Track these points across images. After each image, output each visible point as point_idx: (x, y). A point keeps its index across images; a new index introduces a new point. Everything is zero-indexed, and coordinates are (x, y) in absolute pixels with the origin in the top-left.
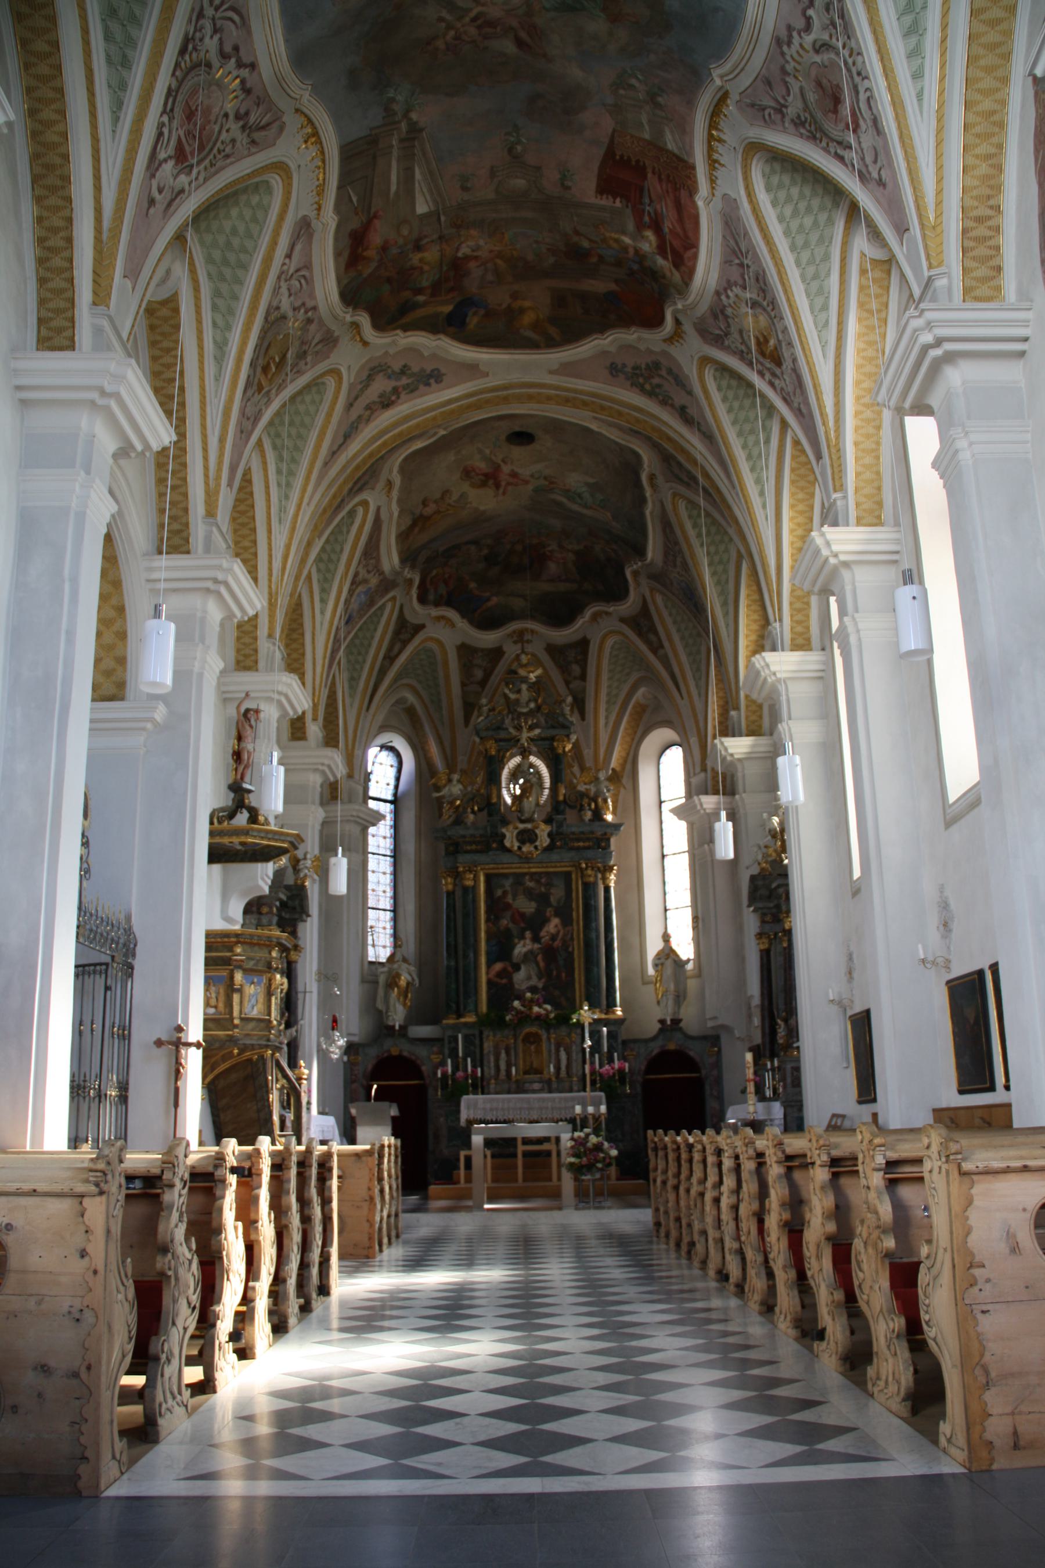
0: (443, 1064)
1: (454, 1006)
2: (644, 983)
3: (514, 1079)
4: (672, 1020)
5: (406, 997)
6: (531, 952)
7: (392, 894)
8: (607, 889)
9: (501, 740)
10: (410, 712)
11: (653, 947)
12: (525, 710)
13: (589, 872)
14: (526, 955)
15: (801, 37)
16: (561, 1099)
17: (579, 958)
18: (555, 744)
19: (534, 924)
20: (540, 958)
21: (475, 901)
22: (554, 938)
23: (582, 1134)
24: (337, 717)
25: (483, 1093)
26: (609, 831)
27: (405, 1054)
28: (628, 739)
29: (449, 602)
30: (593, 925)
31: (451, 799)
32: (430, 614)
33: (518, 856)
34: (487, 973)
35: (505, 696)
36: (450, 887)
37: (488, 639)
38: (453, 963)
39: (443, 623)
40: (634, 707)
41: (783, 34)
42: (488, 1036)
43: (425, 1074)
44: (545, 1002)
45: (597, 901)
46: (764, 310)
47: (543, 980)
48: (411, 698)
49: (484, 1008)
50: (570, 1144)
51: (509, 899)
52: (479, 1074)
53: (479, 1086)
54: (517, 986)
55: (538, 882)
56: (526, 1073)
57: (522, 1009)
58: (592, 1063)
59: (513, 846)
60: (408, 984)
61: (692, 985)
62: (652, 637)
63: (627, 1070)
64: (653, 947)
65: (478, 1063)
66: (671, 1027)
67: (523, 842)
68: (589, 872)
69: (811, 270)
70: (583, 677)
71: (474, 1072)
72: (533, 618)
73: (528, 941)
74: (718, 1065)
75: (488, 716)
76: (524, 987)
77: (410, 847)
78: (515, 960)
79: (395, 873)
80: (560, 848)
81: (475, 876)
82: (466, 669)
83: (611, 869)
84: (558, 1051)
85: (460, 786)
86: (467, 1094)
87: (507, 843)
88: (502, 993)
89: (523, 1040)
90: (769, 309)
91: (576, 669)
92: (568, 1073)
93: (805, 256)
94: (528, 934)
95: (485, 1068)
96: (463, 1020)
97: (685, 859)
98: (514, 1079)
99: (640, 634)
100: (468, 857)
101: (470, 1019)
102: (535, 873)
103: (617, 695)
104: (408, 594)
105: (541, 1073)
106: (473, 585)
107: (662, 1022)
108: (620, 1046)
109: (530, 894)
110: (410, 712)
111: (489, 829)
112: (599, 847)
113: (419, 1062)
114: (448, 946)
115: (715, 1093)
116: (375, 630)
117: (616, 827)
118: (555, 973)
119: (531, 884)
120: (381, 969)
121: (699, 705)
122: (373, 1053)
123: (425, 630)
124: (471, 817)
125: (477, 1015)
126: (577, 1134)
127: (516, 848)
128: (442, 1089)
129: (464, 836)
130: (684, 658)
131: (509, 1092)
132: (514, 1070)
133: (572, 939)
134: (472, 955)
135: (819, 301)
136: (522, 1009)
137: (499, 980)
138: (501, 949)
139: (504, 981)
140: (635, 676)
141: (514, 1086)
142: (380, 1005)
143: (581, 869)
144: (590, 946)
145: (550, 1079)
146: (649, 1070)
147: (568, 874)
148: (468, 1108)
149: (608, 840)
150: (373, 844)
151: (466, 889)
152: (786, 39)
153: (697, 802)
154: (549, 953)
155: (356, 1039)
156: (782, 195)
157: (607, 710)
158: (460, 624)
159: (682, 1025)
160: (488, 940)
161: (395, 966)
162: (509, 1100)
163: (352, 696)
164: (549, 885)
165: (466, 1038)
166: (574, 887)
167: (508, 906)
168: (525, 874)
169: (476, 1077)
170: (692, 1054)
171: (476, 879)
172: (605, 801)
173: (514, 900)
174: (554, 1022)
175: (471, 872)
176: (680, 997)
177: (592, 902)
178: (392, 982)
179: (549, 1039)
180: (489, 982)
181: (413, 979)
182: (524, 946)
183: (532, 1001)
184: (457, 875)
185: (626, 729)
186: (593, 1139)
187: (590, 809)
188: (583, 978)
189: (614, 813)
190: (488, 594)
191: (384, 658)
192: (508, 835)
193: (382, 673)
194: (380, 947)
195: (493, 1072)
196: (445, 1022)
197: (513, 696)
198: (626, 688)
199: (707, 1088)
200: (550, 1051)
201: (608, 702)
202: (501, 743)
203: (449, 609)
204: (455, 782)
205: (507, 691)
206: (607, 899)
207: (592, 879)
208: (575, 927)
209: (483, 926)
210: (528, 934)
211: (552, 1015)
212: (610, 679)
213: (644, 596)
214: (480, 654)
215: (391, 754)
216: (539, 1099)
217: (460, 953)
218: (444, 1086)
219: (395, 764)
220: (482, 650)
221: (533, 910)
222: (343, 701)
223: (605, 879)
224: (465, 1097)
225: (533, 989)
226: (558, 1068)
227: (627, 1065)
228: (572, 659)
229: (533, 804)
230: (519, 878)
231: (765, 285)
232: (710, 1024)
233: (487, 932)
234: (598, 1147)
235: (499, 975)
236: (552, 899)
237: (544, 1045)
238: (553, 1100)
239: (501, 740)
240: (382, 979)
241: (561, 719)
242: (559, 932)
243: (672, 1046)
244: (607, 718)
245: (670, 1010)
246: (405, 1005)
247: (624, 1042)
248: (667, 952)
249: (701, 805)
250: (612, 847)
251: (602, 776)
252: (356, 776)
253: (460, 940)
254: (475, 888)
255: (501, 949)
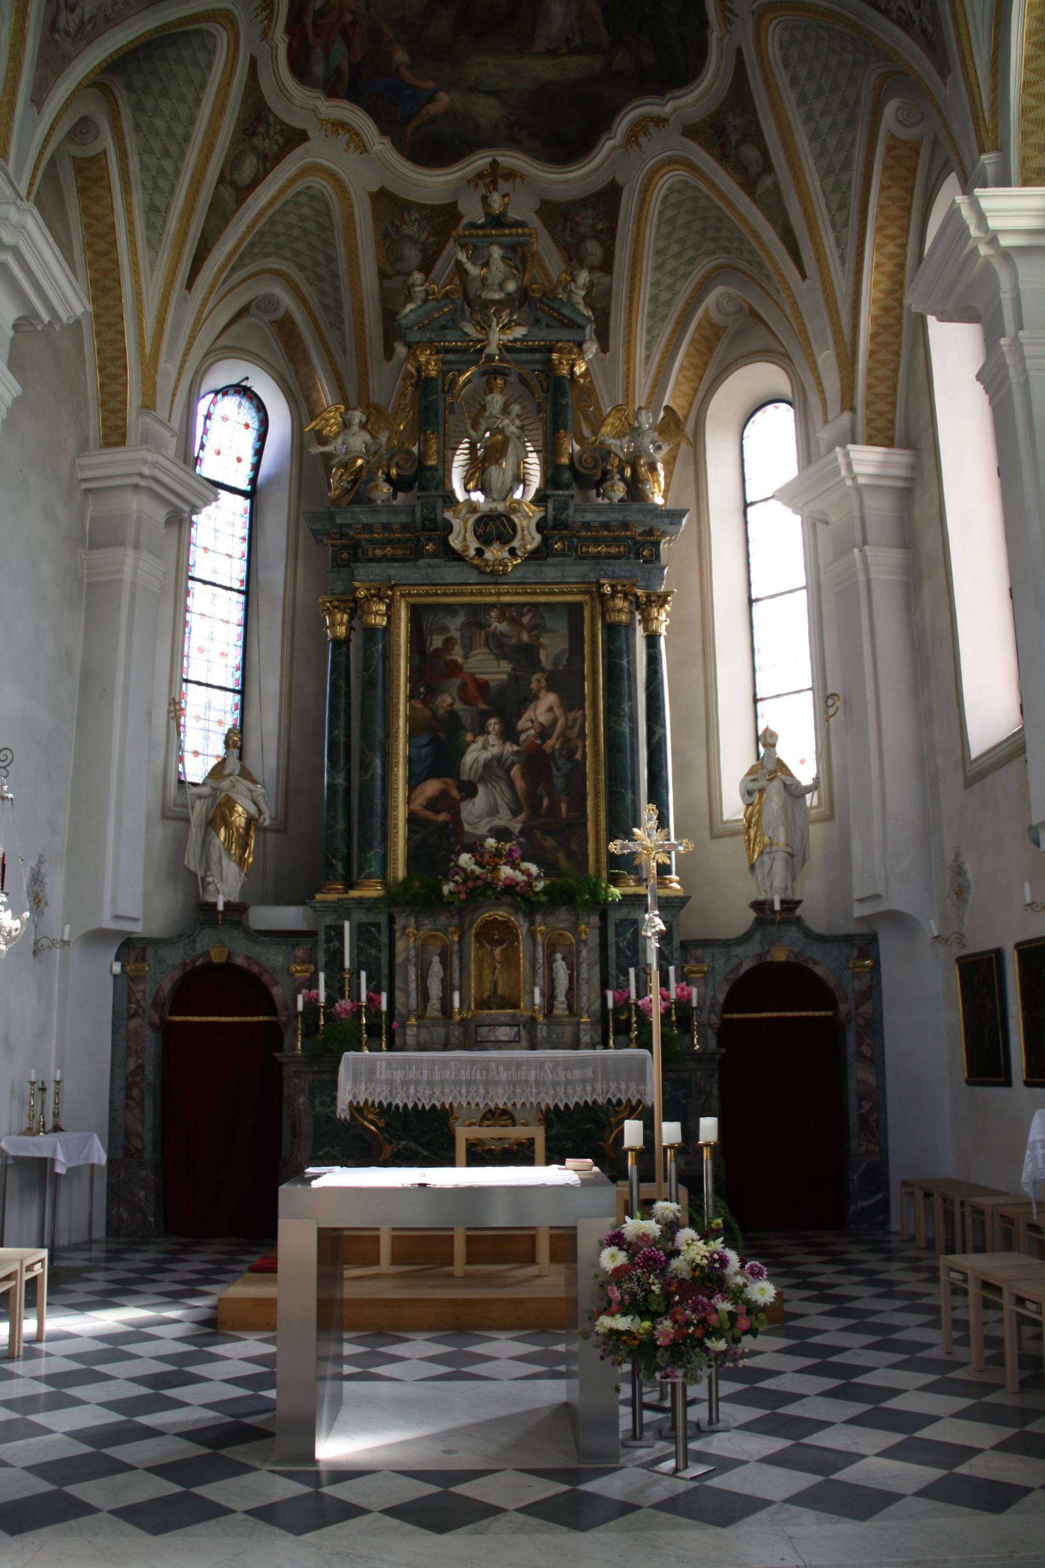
0: (312, 983)
1: (340, 866)
2: (714, 836)
3: (457, 1018)
4: (783, 902)
5: (244, 846)
6: (499, 759)
7: (238, 660)
8: (652, 640)
9: (448, 351)
10: (285, 328)
11: (735, 762)
12: (497, 296)
13: (619, 603)
14: (487, 765)
16: (556, 1063)
17: (597, 772)
18: (555, 356)
19: (506, 705)
20: (515, 772)
21: (388, 657)
22: (545, 733)
23: (652, 1228)
24: (118, 281)
25: (391, 1048)
26: (659, 524)
27: (239, 961)
28: (687, 388)
29: (355, 96)
30: (626, 707)
31: (346, 458)
32: (315, 111)
33: (476, 567)
34: (409, 801)
35: (459, 264)
36: (341, 631)
37: (432, 184)
38: (340, 780)
39: (344, 138)
40: (699, 327)
42: (404, 928)
43: (279, 1003)
44: (525, 859)
45: (632, 662)
47: (522, 817)
48: (287, 301)
49: (400, 870)
50: (611, 1259)
51: (457, 655)
52: (384, 1007)
53: (384, 1032)
54: (467, 828)
55: (515, 622)
56: (482, 1004)
57: (478, 870)
58: (623, 987)
59: (466, 548)
60: (250, 821)
61: (816, 832)
62: (750, 154)
63: (694, 1004)
64: (735, 762)
65: (385, 982)
66: (773, 917)
67: (486, 540)
68: (619, 603)
70: (607, 266)
71: (373, 1002)
72: (512, 142)
73: (492, 738)
74: (872, 993)
75: (425, 301)
76: (482, 829)
77: (275, 575)
78: (465, 777)
79: (246, 624)
80: (562, 554)
81: (389, 607)
82: (390, 241)
83: (662, 600)
84: (550, 961)
85: (367, 437)
86: (359, 1049)
87: (455, 542)
88: (437, 839)
89: (477, 936)
91: (594, 249)
92: (570, 1007)
94: (493, 724)
95: (398, 993)
96: (354, 894)
97: (799, 605)
98: (457, 1018)
99: (724, 155)
100: (376, 572)
101: (373, 891)
102: (510, 605)
103: (669, 303)
104: (265, 35)
105: (515, 1006)
106: (401, 56)
107: (758, 906)
108: (677, 954)
109: (498, 646)
110: (285, 328)
111: (418, 510)
112: (638, 556)
113: (265, 978)
114: (332, 744)
115: (866, 1051)
116: (198, 102)
117: (674, 516)
118: (545, 802)
119: (503, 627)
120: (195, 790)
121: (841, 282)
122: (175, 957)
123: (307, 145)
124: (386, 489)
125: (385, 884)
126: (633, 1226)
127: (472, 552)
128: (305, 1035)
129: (368, 528)
130: (814, 183)
131: (446, 1047)
132: (456, 996)
133: (582, 735)
134: (378, 763)
136: (478, 870)
137: (431, 815)
138: (439, 753)
139: (443, 817)
140: (705, 265)
141: (457, 1032)
142: (192, 861)
143: (602, 596)
144: (617, 749)
145: (533, 1019)
146: (729, 1005)
147: (579, 607)
148: (355, 1079)
149: (657, 544)
150: (201, 564)
151: (370, 632)
153: (841, 459)
154: (536, 762)
155: (137, 929)
157: (650, 330)
158: (378, 147)
159: (799, 912)
160: (411, 736)
161: (225, 784)
162: (444, 1064)
163: (153, 245)
164: (538, 628)
165: (362, 932)
166: (586, 633)
167: (455, 669)
168: (492, 606)
169: (379, 1011)
170: (819, 970)
171: (391, 614)
172: (653, 468)
173: (466, 657)
174: (543, 898)
175: (381, 599)
176: (796, 859)
177: (624, 662)
178: (219, 814)
179: (532, 934)
180: (412, 819)
181: (260, 812)
182: (484, 747)
183: (498, 853)
184: (355, 608)
185: (682, 368)
186: (694, 1248)
187: (623, 479)
188: (603, 815)
189: (665, 497)
190: (429, 85)
191: (221, 180)
192: (457, 524)
193: (218, 218)
194: (202, 749)
195: (413, 1003)
196: (319, 897)
197: (473, 270)
198: (687, 288)
199: (851, 1040)
200: (534, 961)
201: (652, 315)
202: (451, 357)
203: (356, 109)
204: (356, 428)
205: (462, 257)
206: (653, 661)
207: (624, 617)
208: (588, 711)
209: (402, 707)
210: (493, 724)
211: (540, 885)
212: (658, 268)
213: (739, 52)
214: (415, 215)
215: (246, 403)
216: (508, 1063)
217: (355, 758)
218: (311, 1029)
219: (255, 424)
220: (421, 207)
221: (505, 677)
222: (133, 252)
223: (646, 620)
224: (348, 1055)
225: (501, 834)
226: (550, 997)
227: (695, 991)
228: (590, 225)
229: (509, 478)
230: (477, 615)
232: (859, 911)
233: (411, 719)
234: (710, 1278)
235: (433, 804)
236: (542, 658)
237: (523, 948)
238: (540, 1064)
239: (448, 351)
240: (198, 812)
241: (566, 312)
242: (555, 721)
243: (780, 956)
244: (649, 346)
245: (778, 883)
246: (241, 862)
247: (684, 945)
248: (770, 765)
249: (849, 466)
250: (663, 560)
251: (646, 421)
252: (162, 412)
253: (356, 733)
254: (388, 631)
255: (439, 753)
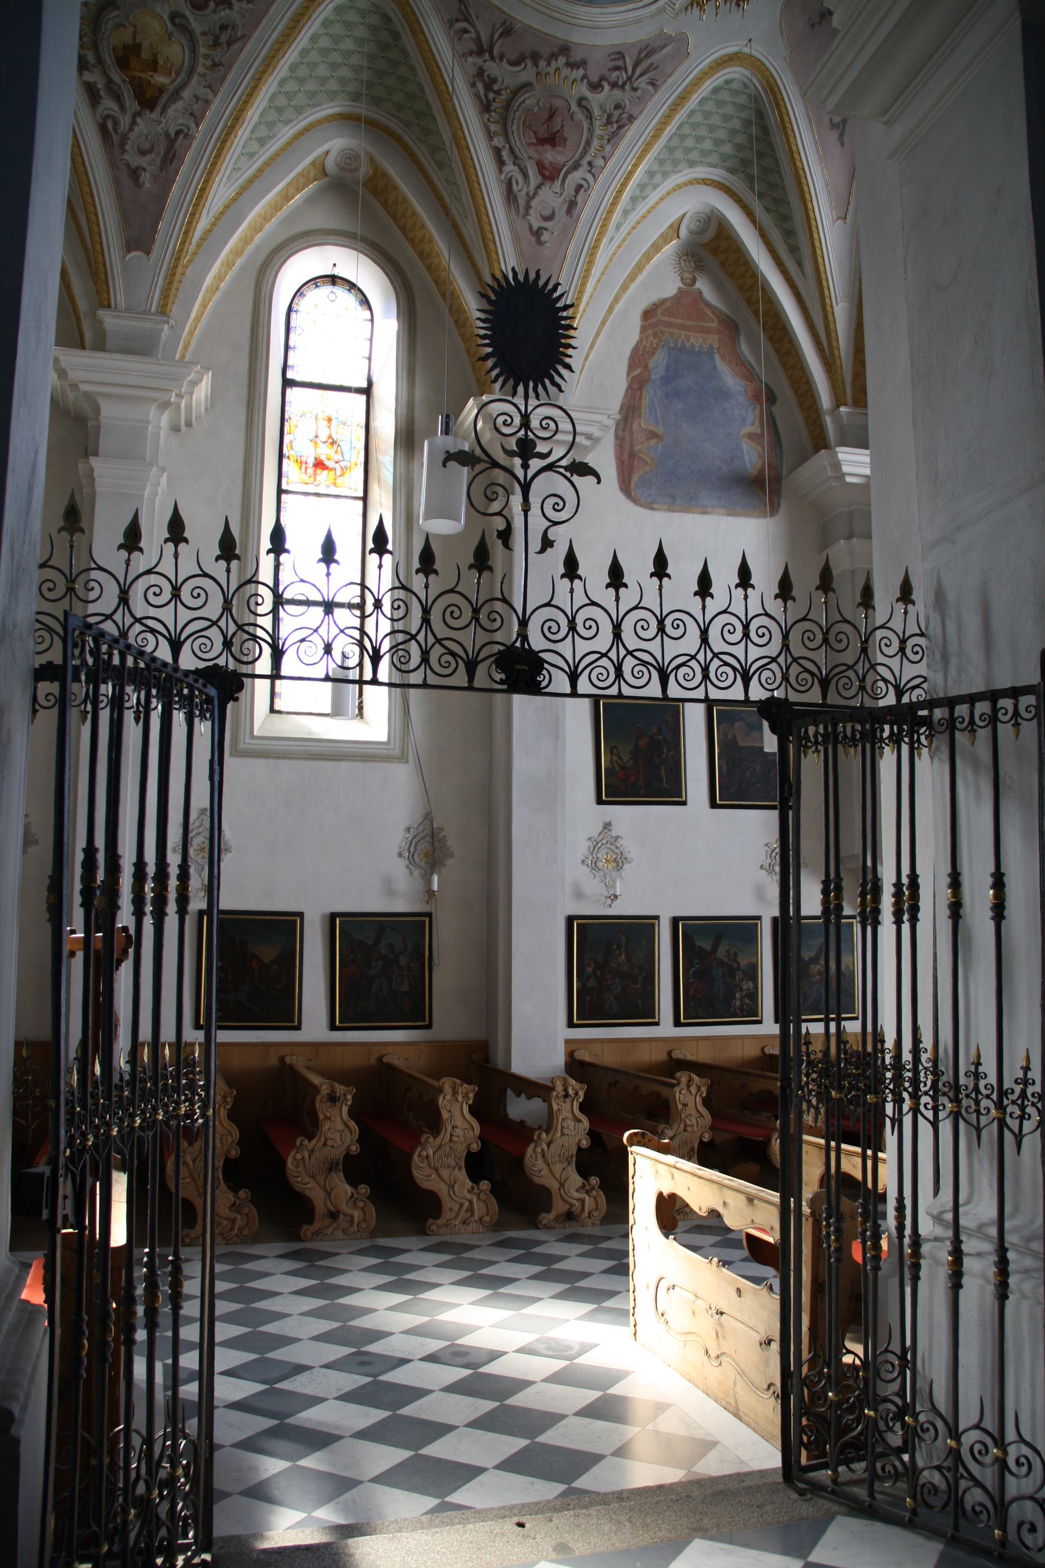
15: (582, 80)
41: (577, 56)
46: (194, 51)
69: (282, 101)
90: (201, 61)
93: (292, 86)
135: (263, 132)
152: (572, 60)
156: (338, 29)
231: (229, 44)
